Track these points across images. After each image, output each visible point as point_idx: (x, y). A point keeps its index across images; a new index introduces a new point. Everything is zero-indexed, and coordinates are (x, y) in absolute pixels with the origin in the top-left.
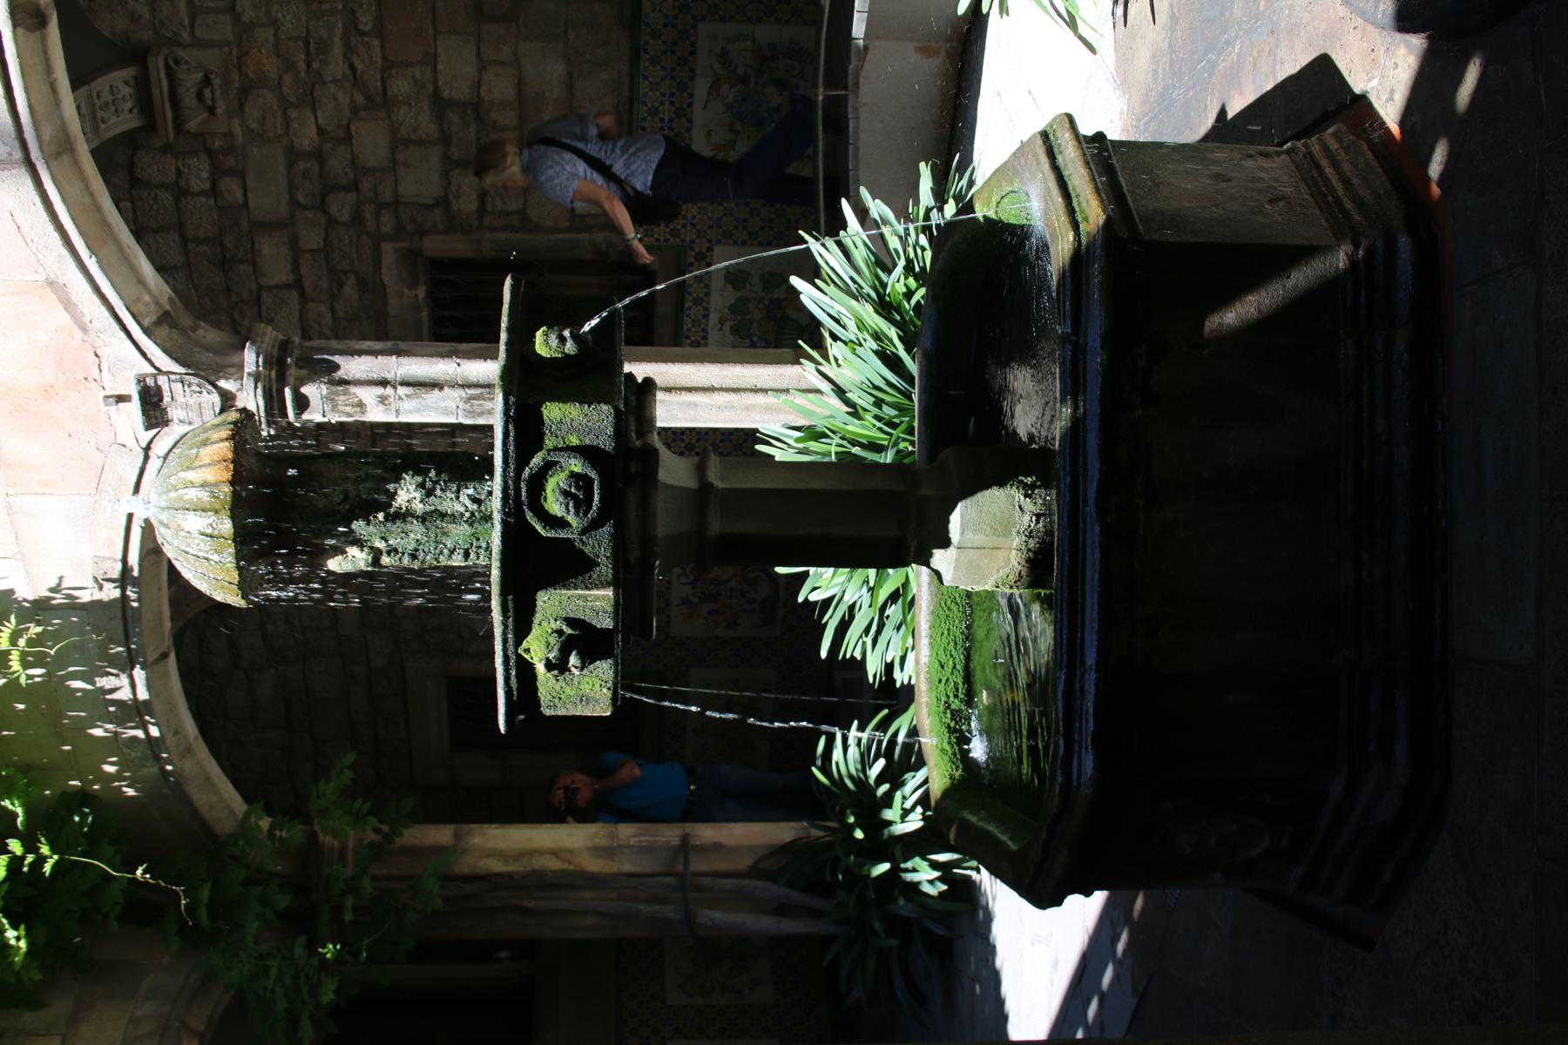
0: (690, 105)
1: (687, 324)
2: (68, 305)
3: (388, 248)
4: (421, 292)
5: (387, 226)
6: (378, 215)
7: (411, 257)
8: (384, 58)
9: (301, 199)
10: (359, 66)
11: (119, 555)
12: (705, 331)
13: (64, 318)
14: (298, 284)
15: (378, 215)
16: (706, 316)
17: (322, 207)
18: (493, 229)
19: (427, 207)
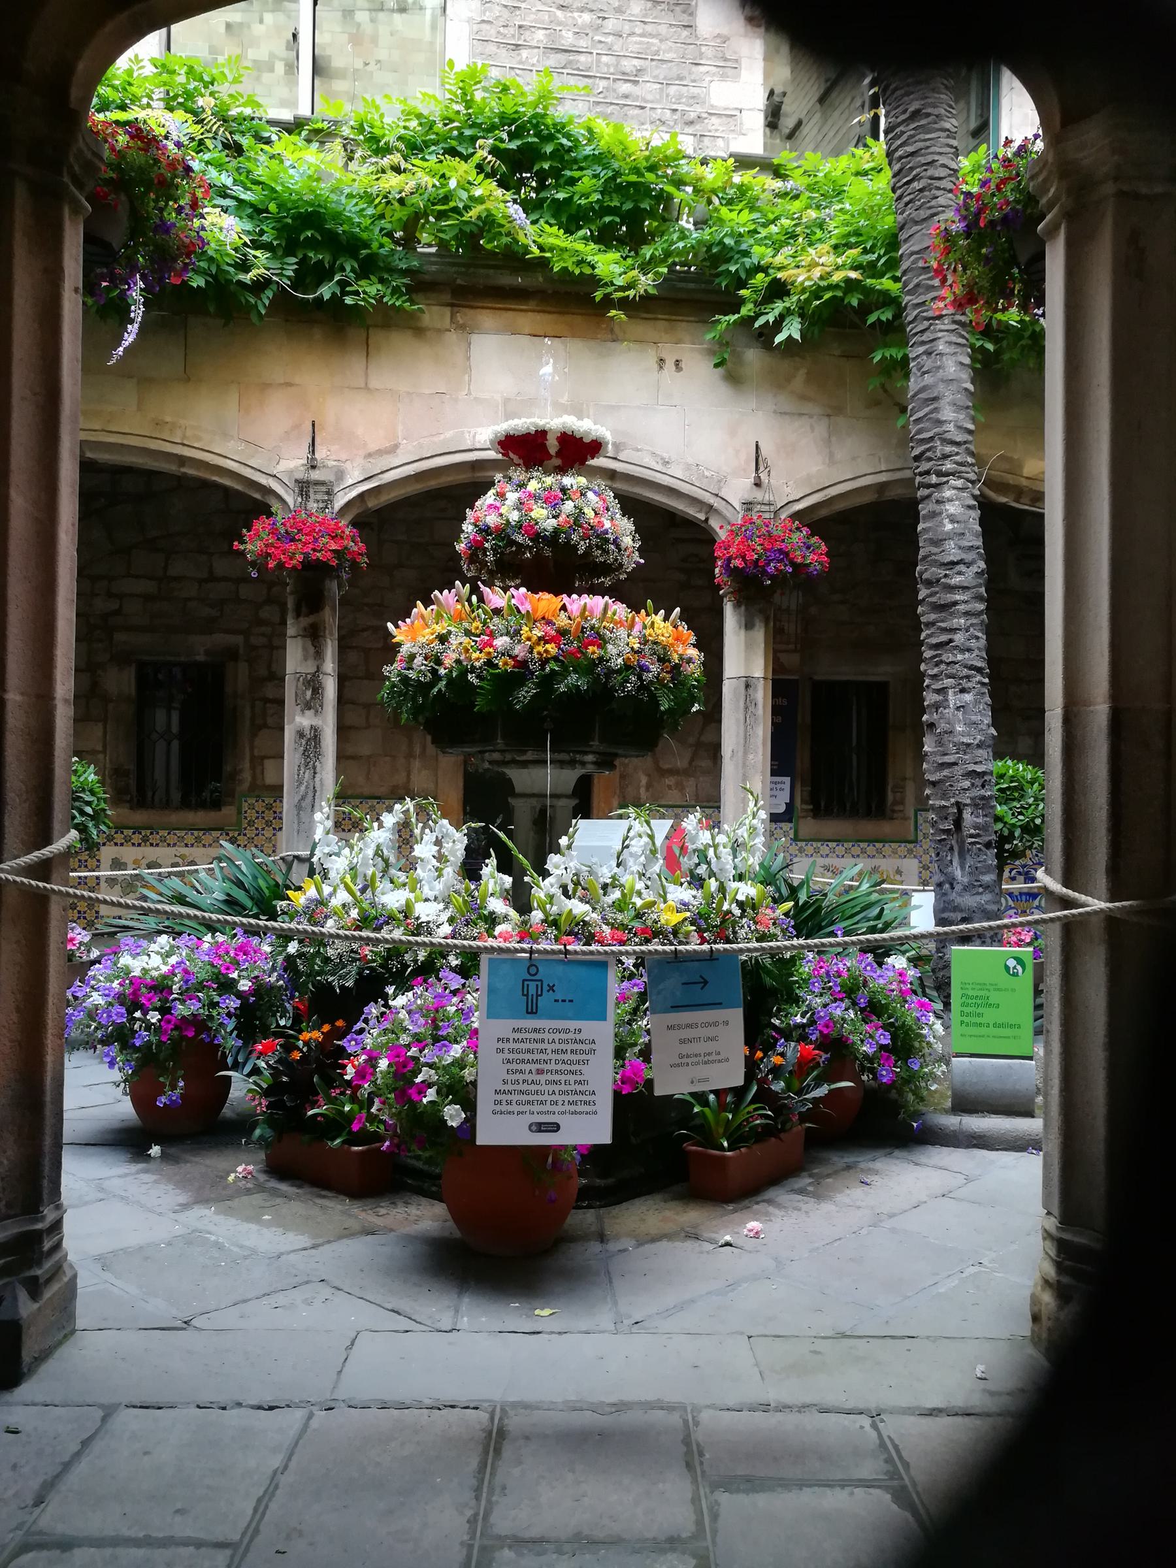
0: (344, 830)
1: (182, 833)
2: (380, 453)
3: (239, 639)
4: (201, 658)
5: (254, 641)
6: (263, 635)
7: (232, 654)
8: (370, 649)
9: (275, 589)
10: (365, 634)
11: (186, 442)
12: (175, 845)
13: (373, 447)
14: (212, 578)
15: (263, 635)
16: (186, 845)
17: (269, 601)
18: (253, 707)
19: (269, 666)
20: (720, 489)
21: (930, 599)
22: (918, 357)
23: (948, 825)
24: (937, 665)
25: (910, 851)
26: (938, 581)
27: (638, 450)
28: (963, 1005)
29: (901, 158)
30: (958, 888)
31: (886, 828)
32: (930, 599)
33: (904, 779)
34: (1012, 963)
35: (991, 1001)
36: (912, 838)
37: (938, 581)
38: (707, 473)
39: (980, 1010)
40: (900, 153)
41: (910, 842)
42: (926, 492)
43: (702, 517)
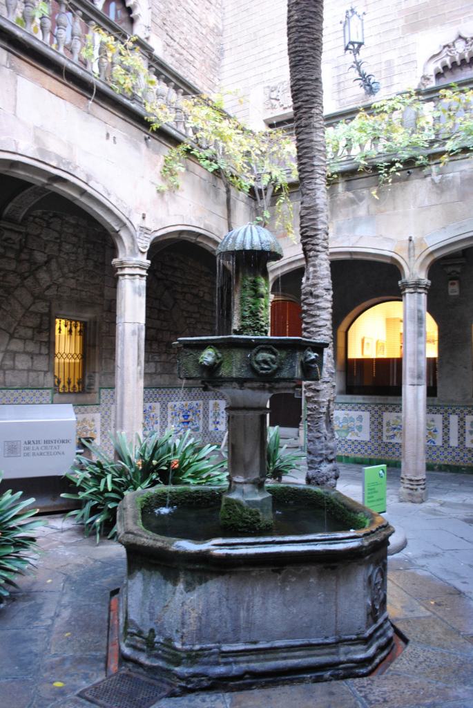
20: (130, 215)
21: (318, 304)
22: (313, 189)
23: (324, 410)
24: (319, 335)
25: (98, 409)
26: (322, 296)
27: (98, 183)
28: (369, 493)
29: (308, 95)
30: (328, 438)
31: (88, 398)
32: (318, 304)
33: (94, 372)
34: (381, 472)
35: (376, 490)
36: (97, 402)
37: (322, 296)
38: (125, 206)
39: (373, 495)
40: (309, 93)
41: (97, 405)
42: (315, 253)
43: (117, 228)
